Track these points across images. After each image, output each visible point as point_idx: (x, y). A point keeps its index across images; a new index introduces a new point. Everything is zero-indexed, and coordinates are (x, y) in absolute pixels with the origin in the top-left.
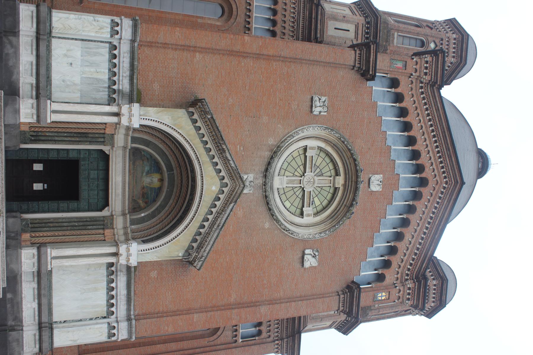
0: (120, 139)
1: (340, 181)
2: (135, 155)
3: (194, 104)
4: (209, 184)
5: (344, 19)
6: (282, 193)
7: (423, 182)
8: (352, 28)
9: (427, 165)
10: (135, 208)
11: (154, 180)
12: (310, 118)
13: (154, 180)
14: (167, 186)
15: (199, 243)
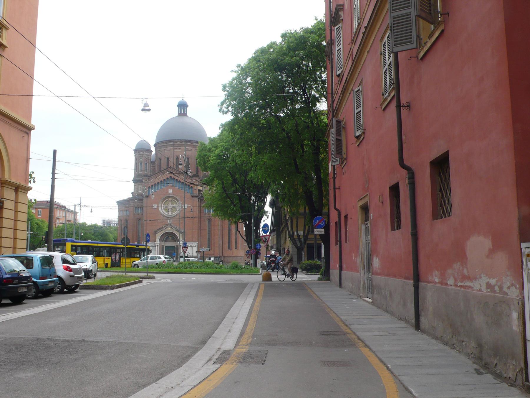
0: (163, 244)
1: (170, 199)
2: (166, 241)
3: (155, 233)
4: (169, 229)
5: (137, 189)
6: (172, 212)
7: (171, 177)
8: (139, 186)
9: (166, 177)
10: (175, 241)
11: (170, 238)
12: (157, 208)
13: (170, 238)
14: (169, 236)
15: (178, 231)
